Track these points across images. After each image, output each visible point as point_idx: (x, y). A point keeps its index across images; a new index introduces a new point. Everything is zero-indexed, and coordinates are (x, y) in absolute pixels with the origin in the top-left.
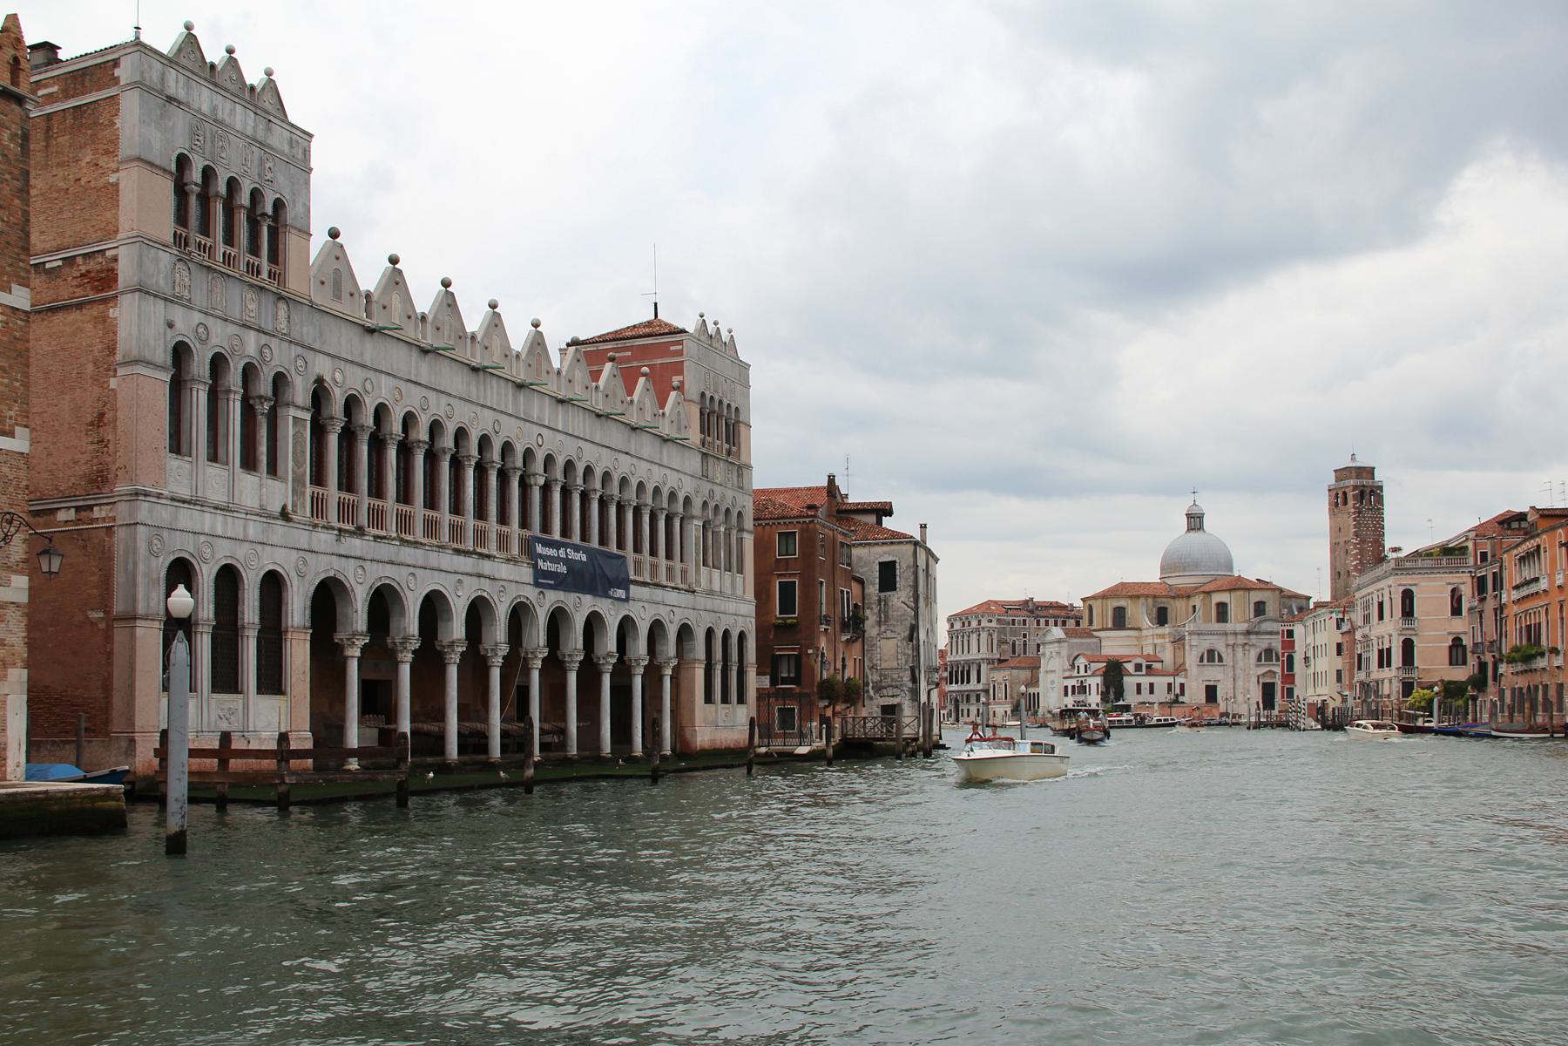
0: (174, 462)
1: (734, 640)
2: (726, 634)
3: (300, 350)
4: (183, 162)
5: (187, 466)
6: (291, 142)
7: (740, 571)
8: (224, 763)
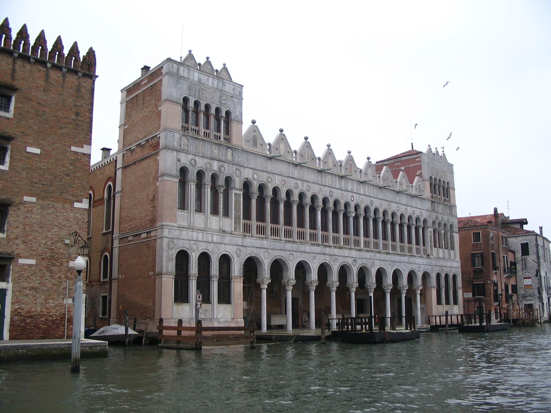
0: (180, 213)
1: (451, 278)
2: (447, 276)
3: (238, 167)
4: (186, 100)
5: (186, 214)
6: (234, 89)
7: (453, 248)
8: (179, 333)
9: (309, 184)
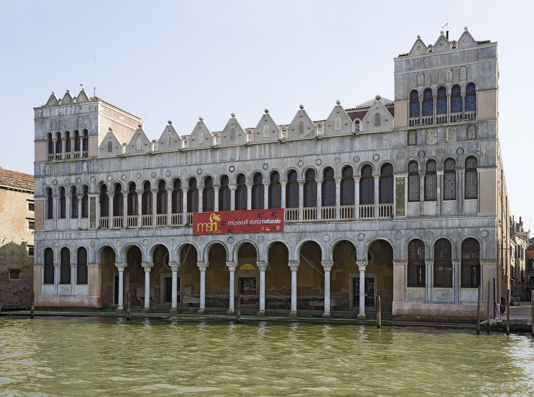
3: (92, 175)
4: (50, 135)
9: (169, 169)
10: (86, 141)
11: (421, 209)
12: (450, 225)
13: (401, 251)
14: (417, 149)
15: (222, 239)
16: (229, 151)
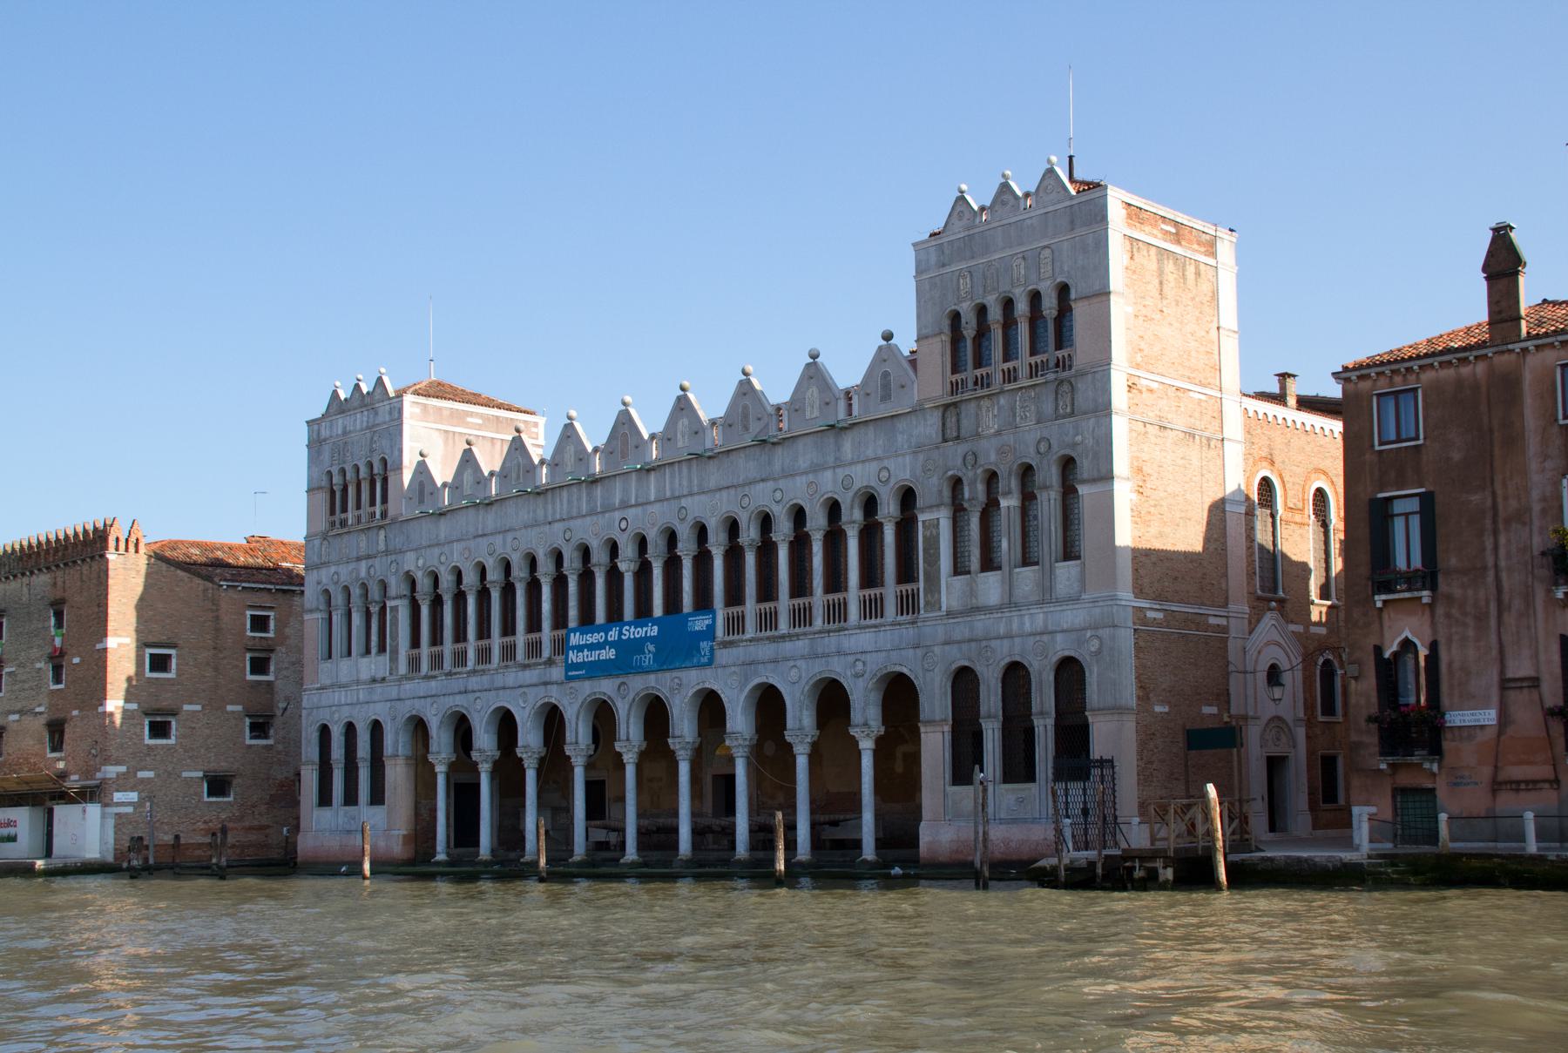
4: (330, 473)
9: (518, 534)
10: (385, 480)
11: (972, 593)
12: (1028, 627)
13: (935, 702)
14: (962, 448)
15: (606, 687)
16: (618, 484)
